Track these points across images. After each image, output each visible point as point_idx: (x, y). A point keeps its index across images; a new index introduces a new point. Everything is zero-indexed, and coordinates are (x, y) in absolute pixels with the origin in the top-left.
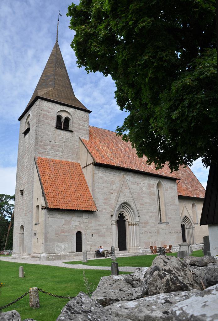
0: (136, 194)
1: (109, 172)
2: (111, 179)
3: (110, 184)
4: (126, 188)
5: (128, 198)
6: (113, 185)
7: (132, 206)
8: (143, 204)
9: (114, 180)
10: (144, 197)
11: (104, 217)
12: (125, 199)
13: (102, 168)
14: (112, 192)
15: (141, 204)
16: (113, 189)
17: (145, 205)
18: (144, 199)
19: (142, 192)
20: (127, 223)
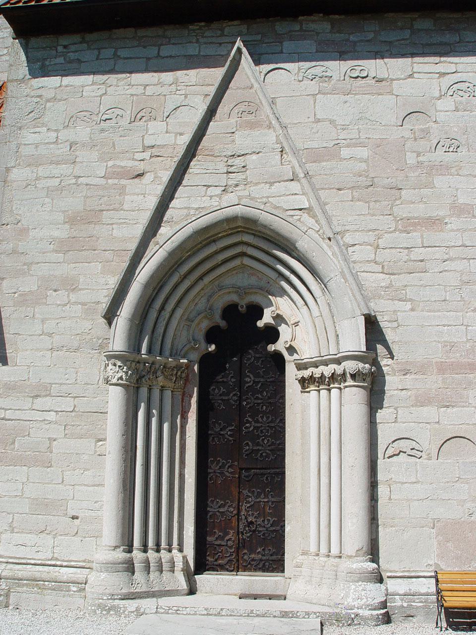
0: (363, 152)
1: (123, 53)
2: (140, 90)
3: (125, 122)
4: (252, 126)
5: (261, 191)
6: (151, 124)
7: (303, 244)
8: (434, 223)
9: (165, 90)
10: (444, 169)
11: (50, 335)
12: (231, 198)
13: (77, 38)
14: (141, 167)
15: (409, 225)
16: (145, 148)
17: (455, 223)
18: (440, 182)
19: (426, 132)
20: (292, 374)
